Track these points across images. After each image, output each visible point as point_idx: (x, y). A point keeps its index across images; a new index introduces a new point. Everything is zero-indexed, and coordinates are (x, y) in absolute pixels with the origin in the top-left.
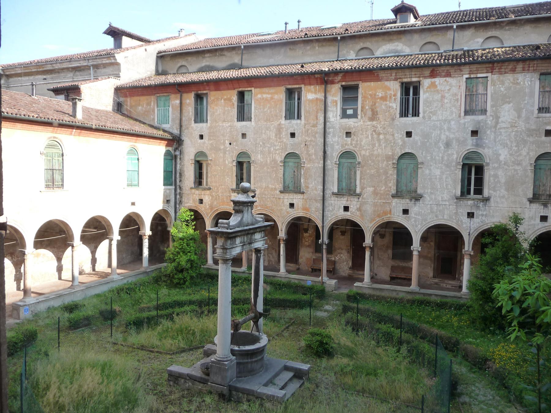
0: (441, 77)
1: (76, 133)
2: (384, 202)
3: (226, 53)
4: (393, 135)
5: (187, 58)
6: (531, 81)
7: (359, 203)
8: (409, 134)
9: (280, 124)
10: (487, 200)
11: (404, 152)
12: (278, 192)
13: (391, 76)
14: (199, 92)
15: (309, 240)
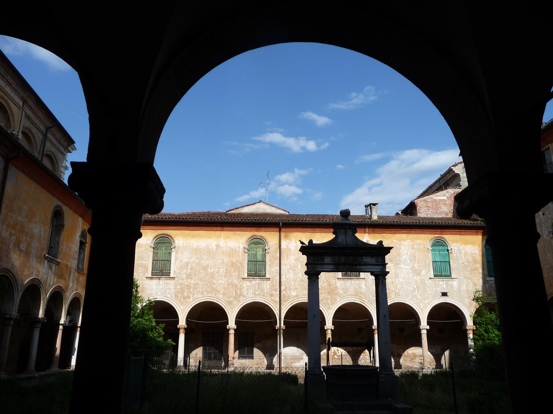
1: (369, 231)
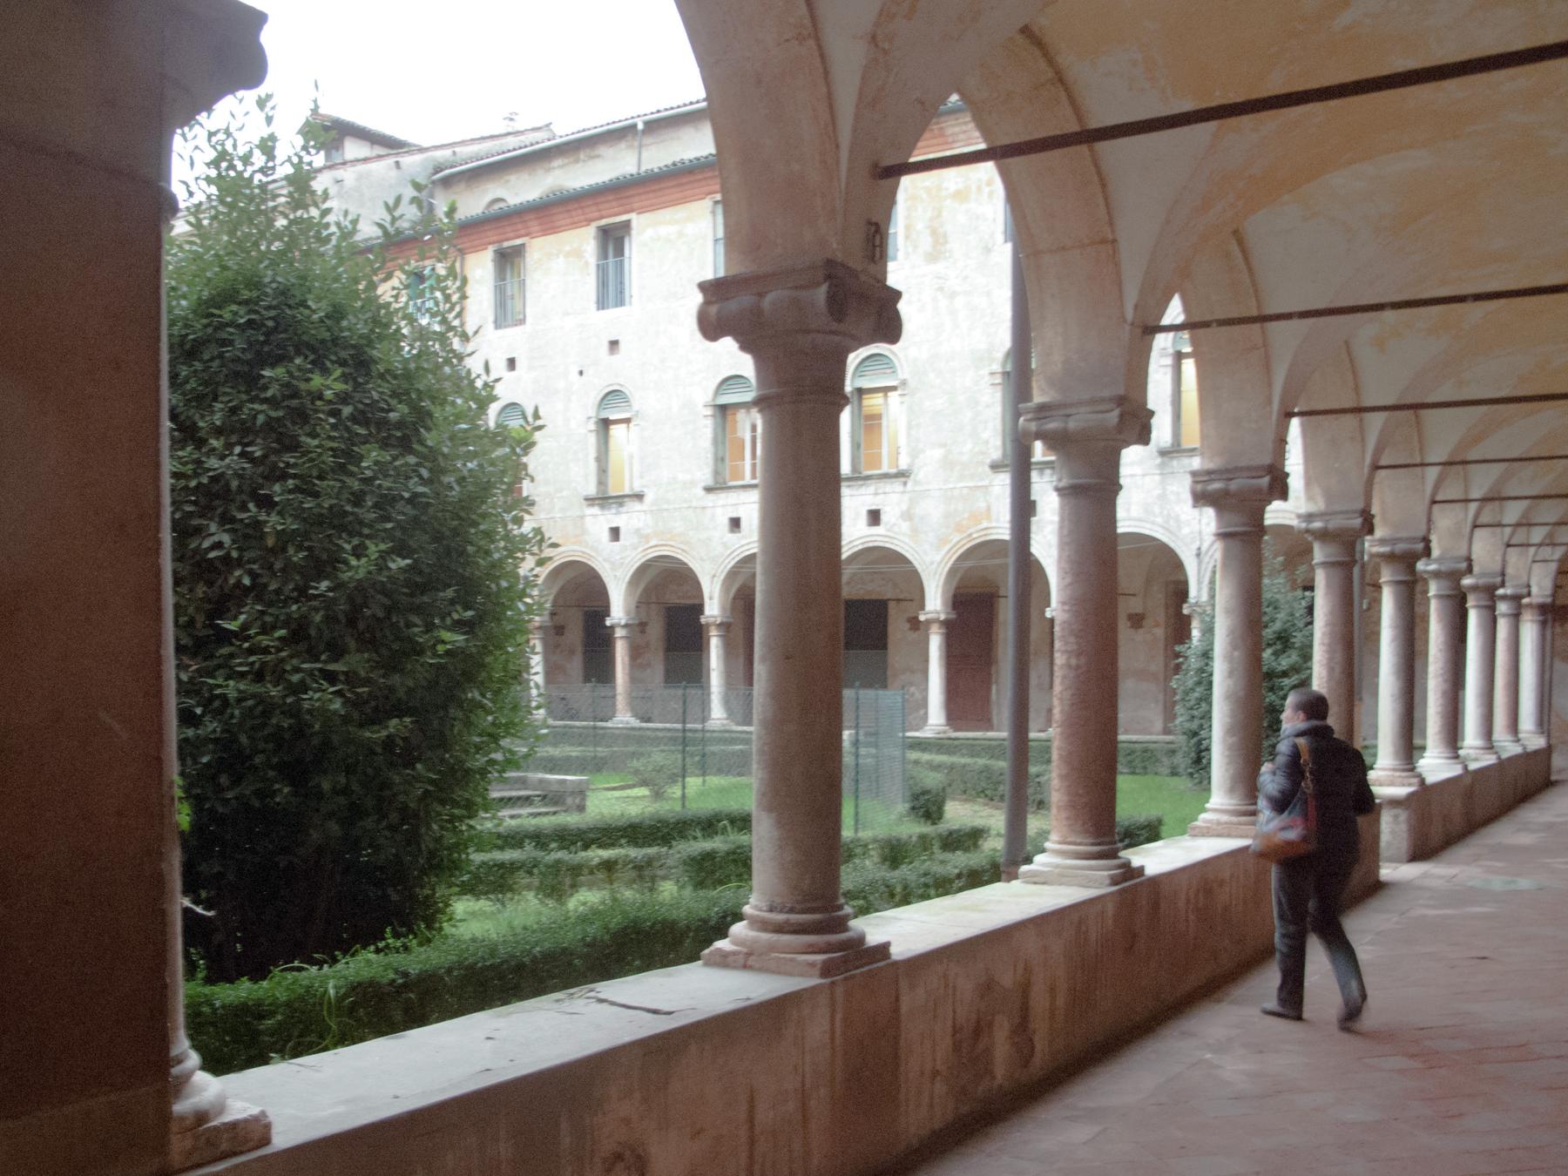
3: (603, 150)
5: (507, 178)
7: (906, 497)
14: (506, 244)
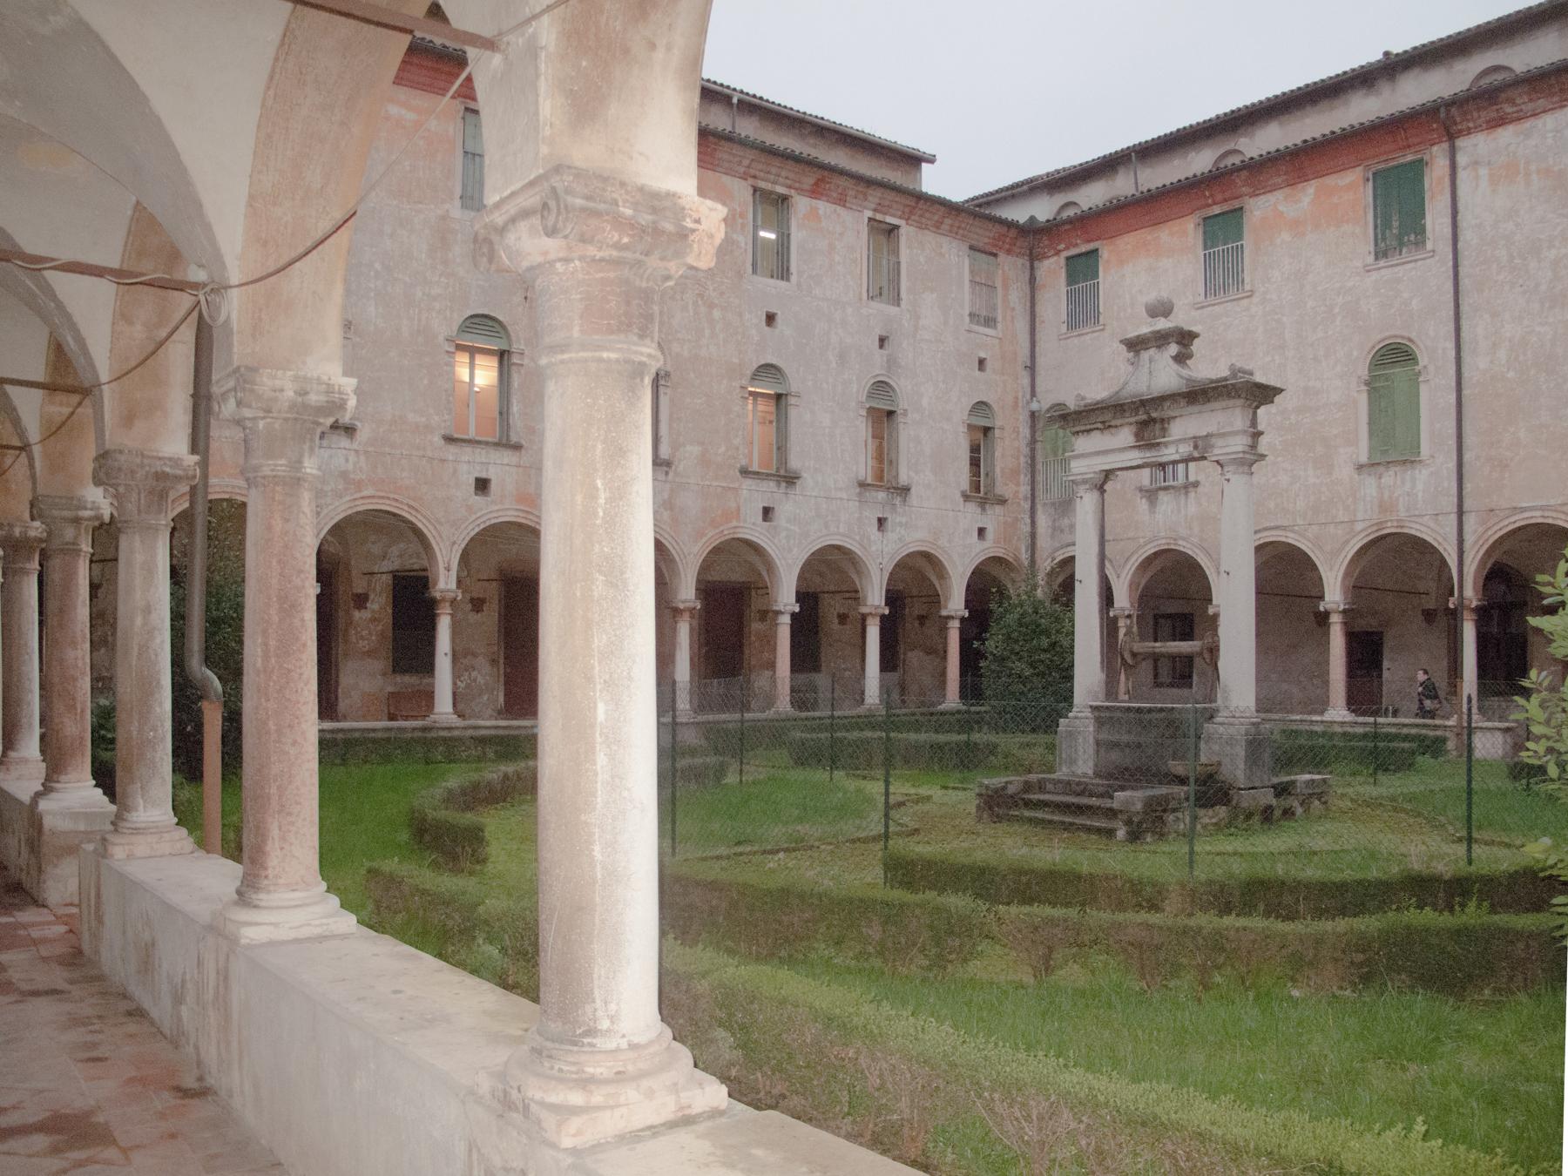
0: (828, 201)
2: (723, 487)
4: (741, 315)
6: (958, 256)
7: (668, 486)
8: (770, 319)
9: (444, 218)
10: (906, 490)
11: (763, 362)
12: (437, 440)
13: (740, 163)
15: (370, 634)
